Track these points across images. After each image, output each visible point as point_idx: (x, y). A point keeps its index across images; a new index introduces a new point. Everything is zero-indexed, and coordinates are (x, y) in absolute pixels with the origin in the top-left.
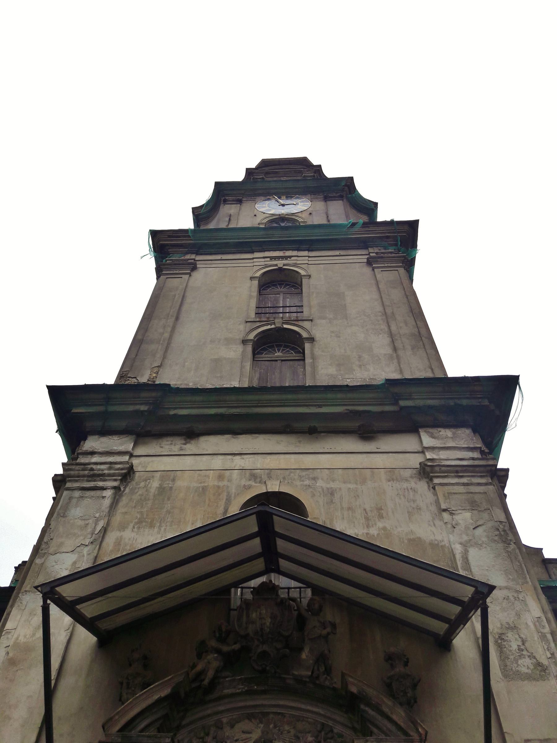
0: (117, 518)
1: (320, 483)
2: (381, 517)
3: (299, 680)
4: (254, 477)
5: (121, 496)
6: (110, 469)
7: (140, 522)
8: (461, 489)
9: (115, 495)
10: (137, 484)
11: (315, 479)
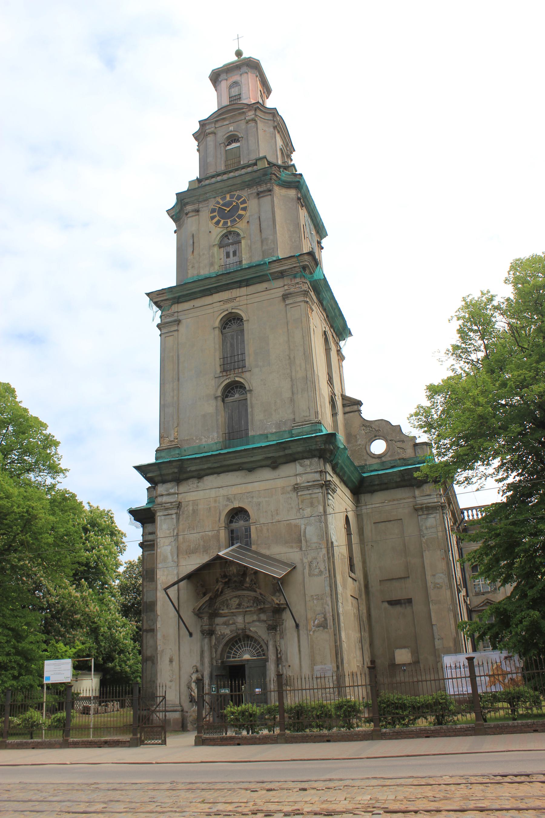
0: (181, 527)
1: (255, 500)
2: (277, 514)
3: (246, 587)
4: (228, 499)
5: (179, 515)
6: (171, 505)
7: (189, 528)
8: (308, 497)
9: (176, 516)
10: (184, 508)
11: (252, 497)
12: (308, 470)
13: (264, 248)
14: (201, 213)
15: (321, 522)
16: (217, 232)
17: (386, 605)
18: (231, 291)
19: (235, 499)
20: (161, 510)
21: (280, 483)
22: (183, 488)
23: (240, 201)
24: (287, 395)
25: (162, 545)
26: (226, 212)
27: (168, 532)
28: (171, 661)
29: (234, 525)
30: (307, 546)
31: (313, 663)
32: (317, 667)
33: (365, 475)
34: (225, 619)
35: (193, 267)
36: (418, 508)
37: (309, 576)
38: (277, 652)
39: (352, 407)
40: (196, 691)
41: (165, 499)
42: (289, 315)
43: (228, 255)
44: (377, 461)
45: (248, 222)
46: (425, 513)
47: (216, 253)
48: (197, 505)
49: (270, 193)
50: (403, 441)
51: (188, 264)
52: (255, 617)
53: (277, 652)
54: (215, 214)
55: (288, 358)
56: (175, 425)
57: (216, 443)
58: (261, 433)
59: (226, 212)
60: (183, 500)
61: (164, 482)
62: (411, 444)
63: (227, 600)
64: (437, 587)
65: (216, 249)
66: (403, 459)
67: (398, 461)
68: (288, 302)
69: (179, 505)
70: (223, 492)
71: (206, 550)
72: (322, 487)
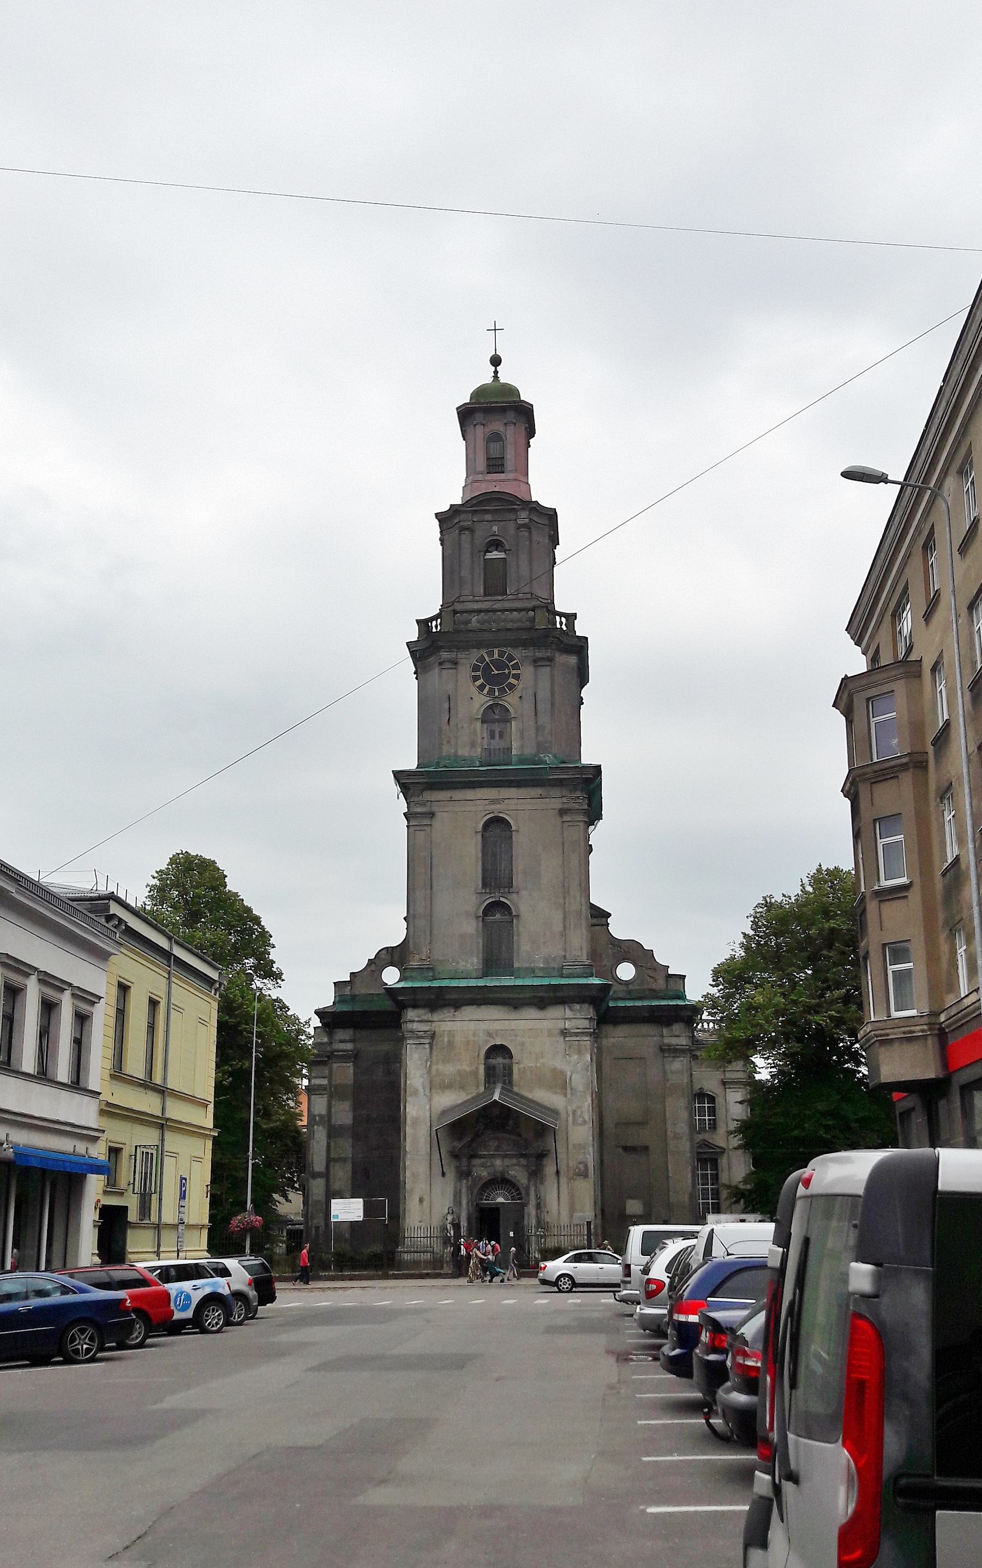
0: (434, 1058)
1: (519, 1038)
2: (542, 1057)
4: (489, 1035)
11: (516, 1036)
12: (578, 1015)
13: (540, 738)
14: (460, 667)
15: (587, 1071)
16: (480, 701)
17: (621, 1150)
18: (499, 788)
19: (496, 1035)
20: (411, 1038)
21: (546, 1024)
22: (436, 1017)
23: (511, 664)
24: (558, 927)
25: (412, 1076)
26: (493, 673)
27: (420, 1062)
28: (421, 1200)
29: (493, 1062)
30: (572, 1094)
31: (572, 1210)
32: (577, 1214)
33: (611, 1004)
34: (482, 1160)
35: (448, 742)
36: (665, 1049)
37: (573, 1124)
38: (538, 1198)
39: (599, 919)
40: (452, 1232)
41: (415, 1026)
42: (565, 833)
43: (492, 736)
44: (623, 988)
45: (520, 697)
46: (672, 1055)
47: (479, 731)
48: (454, 1037)
49: (549, 663)
50: (655, 970)
51: (443, 737)
52: (514, 1161)
53: (538, 1198)
54: (478, 673)
55: (561, 885)
56: (428, 941)
57: (476, 970)
58: (527, 966)
59: (493, 673)
60: (437, 1029)
61: (415, 1006)
62: (663, 974)
63: (485, 1141)
64: (677, 1137)
65: (479, 724)
66: (654, 990)
67: (647, 992)
68: (566, 818)
69: (433, 1036)
70: (483, 1026)
71: (462, 1087)
72: (591, 1035)
